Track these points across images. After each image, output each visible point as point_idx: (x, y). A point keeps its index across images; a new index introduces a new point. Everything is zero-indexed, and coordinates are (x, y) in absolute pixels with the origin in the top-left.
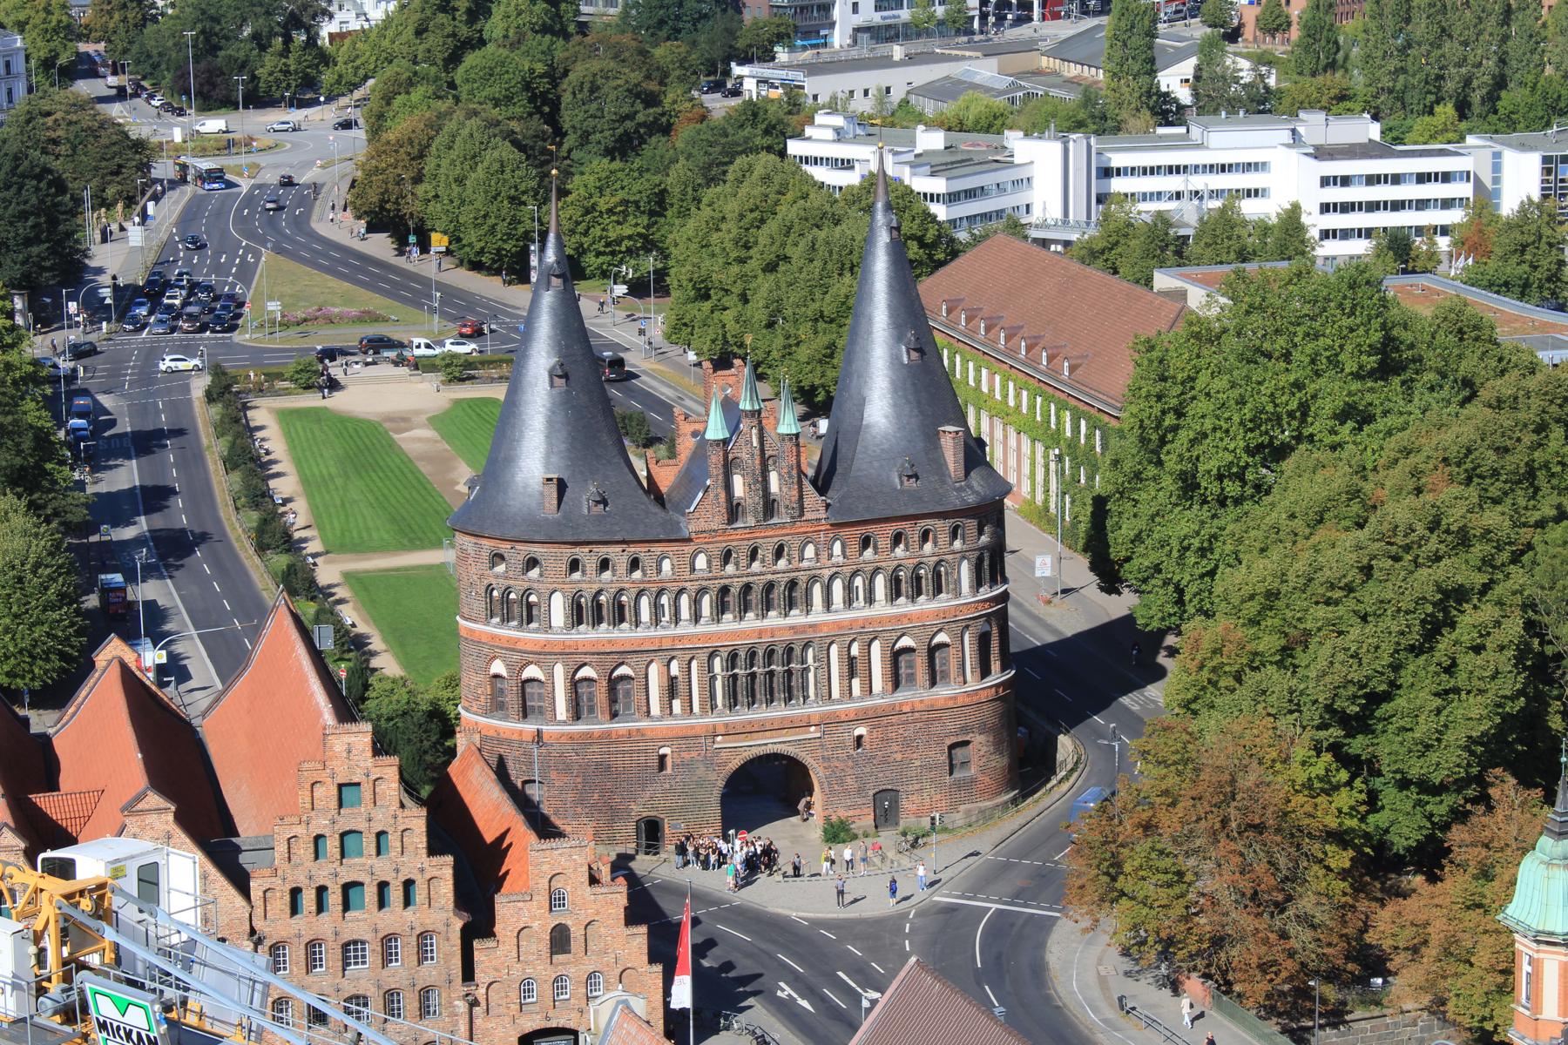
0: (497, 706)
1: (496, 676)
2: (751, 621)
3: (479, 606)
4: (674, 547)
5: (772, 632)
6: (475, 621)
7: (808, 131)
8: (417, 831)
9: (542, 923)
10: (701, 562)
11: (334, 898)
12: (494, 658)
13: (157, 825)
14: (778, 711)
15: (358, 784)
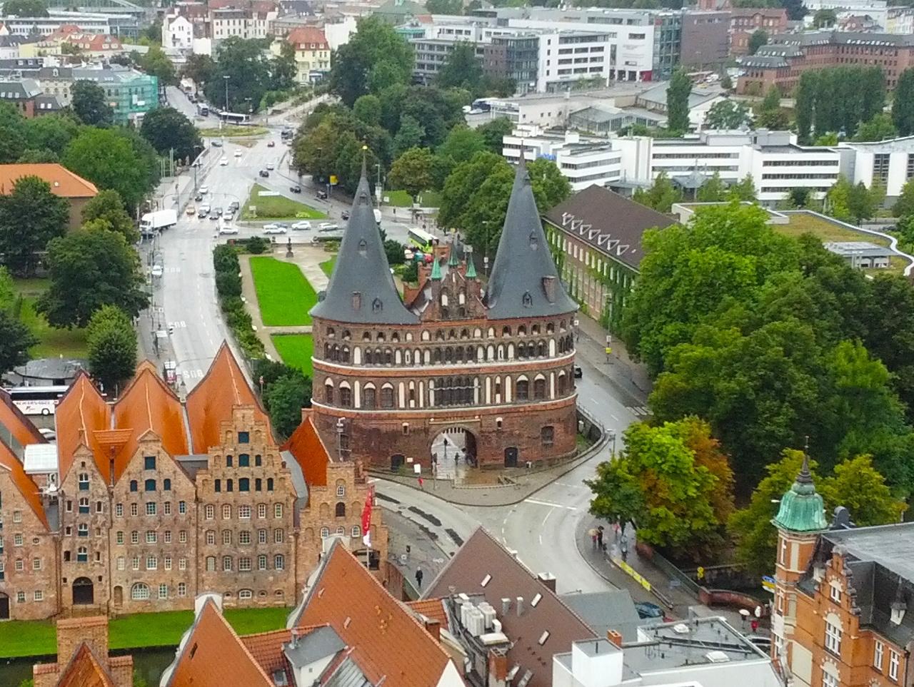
0: (329, 400)
1: (328, 386)
2: (449, 366)
3: (322, 352)
5: (459, 370)
6: (320, 359)
7: (514, 132)
9: (332, 503)
11: (236, 485)
12: (327, 377)
13: (154, 447)
14: (461, 409)
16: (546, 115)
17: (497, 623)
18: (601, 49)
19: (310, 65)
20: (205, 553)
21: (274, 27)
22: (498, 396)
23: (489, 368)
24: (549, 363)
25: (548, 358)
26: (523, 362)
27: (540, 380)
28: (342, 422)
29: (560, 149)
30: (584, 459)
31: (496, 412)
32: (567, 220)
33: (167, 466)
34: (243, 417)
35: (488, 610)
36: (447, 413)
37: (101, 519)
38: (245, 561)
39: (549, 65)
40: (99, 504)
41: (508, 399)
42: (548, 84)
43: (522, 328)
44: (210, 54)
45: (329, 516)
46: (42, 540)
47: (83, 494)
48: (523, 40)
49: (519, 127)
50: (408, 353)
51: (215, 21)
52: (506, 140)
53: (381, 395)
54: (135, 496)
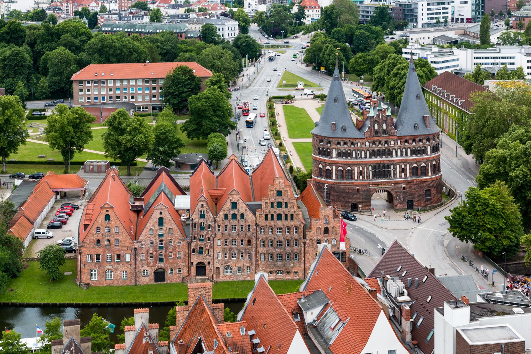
0: (320, 175)
1: (320, 168)
2: (379, 159)
3: (317, 152)
5: (383, 161)
7: (407, 47)
9: (322, 227)
11: (275, 217)
16: (422, 39)
17: (405, 290)
19: (312, 15)
22: (403, 174)
24: (428, 158)
25: (427, 155)
26: (414, 157)
27: (423, 166)
28: (327, 186)
30: (446, 206)
33: (242, 207)
37: (210, 233)
38: (279, 256)
40: (209, 225)
42: (423, 24)
43: (414, 141)
45: (321, 233)
46: (182, 243)
47: (202, 220)
49: (410, 44)
50: (358, 152)
52: (404, 50)
54: (226, 222)
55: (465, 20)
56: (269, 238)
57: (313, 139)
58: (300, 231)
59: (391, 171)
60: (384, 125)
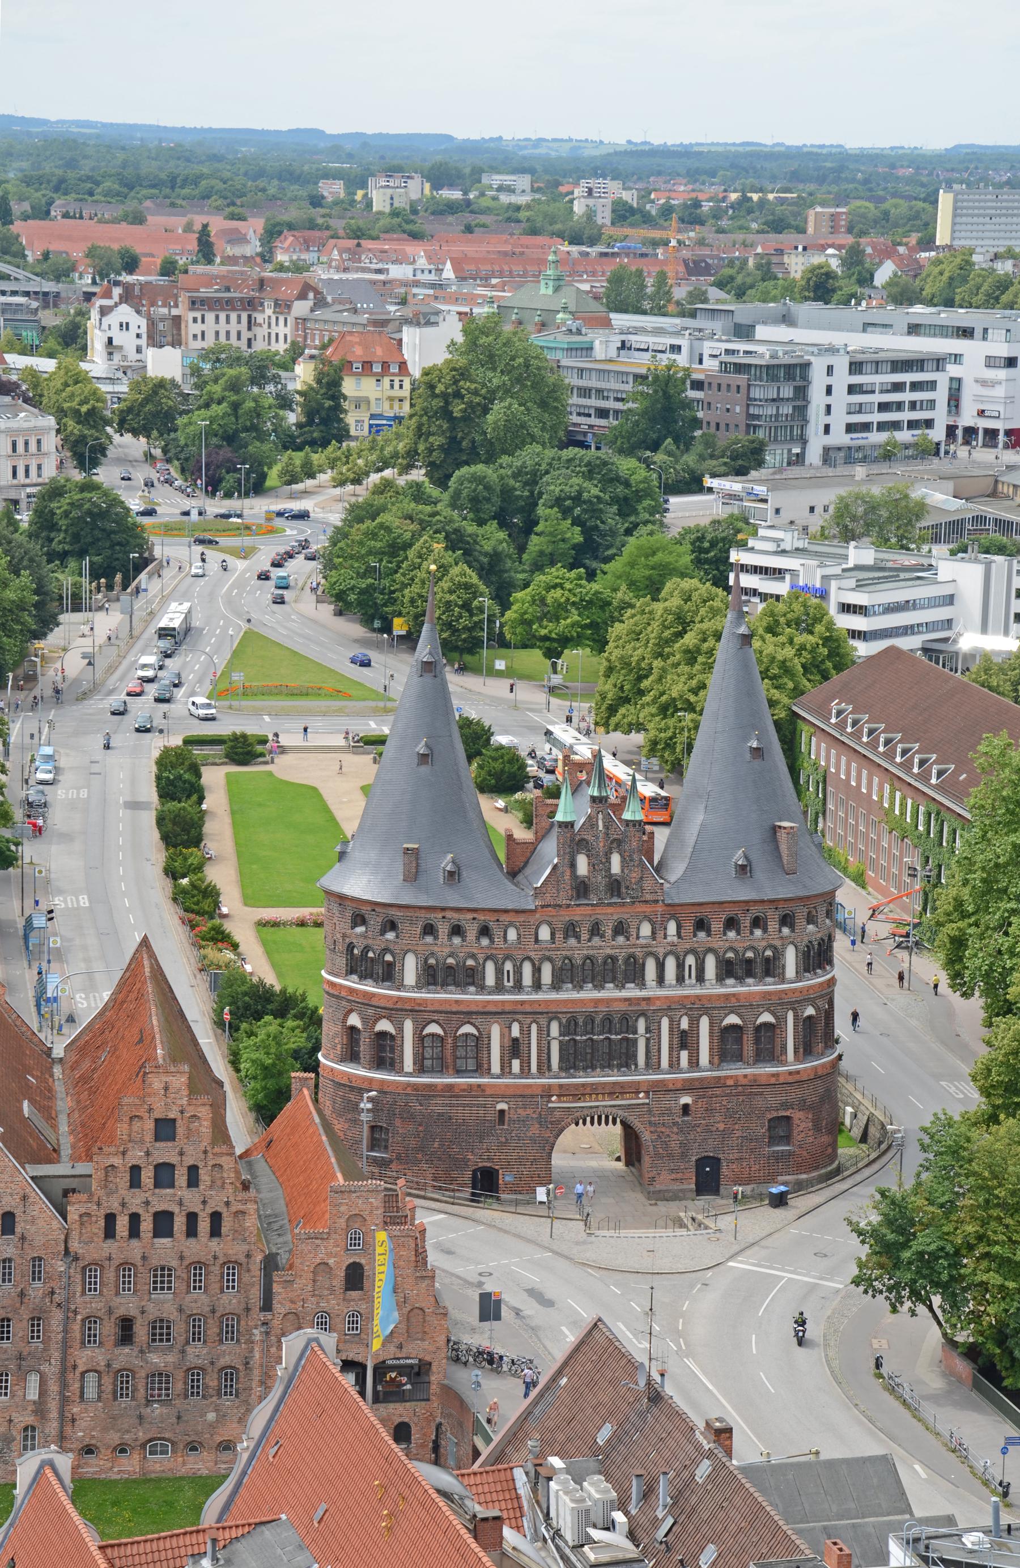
0: (352, 1056)
1: (353, 1028)
2: (589, 993)
3: (342, 962)
4: (522, 918)
5: (608, 1001)
8: (226, 1167)
9: (339, 1264)
10: (545, 933)
11: (147, 1225)
12: (351, 1011)
15: (174, 1120)
18: (932, 385)
20: (79, 1362)
21: (305, 329)
22: (684, 1055)
23: (667, 998)
24: (785, 992)
25: (783, 981)
26: (731, 987)
27: (766, 1025)
28: (371, 1100)
29: (836, 577)
31: (679, 1086)
32: (839, 713)
34: (166, 1089)
35: (597, 1489)
36: (583, 1085)
39: (830, 411)
41: (704, 1058)
42: (827, 450)
43: (731, 923)
44: (179, 379)
45: (332, 1289)
48: (779, 366)
49: (761, 532)
50: (508, 966)
51: (192, 315)
52: (735, 556)
53: (455, 1047)
55: (1001, 438)
56: (121, 1312)
57: (329, 910)
58: (246, 1278)
59: (635, 1041)
60: (616, 860)
